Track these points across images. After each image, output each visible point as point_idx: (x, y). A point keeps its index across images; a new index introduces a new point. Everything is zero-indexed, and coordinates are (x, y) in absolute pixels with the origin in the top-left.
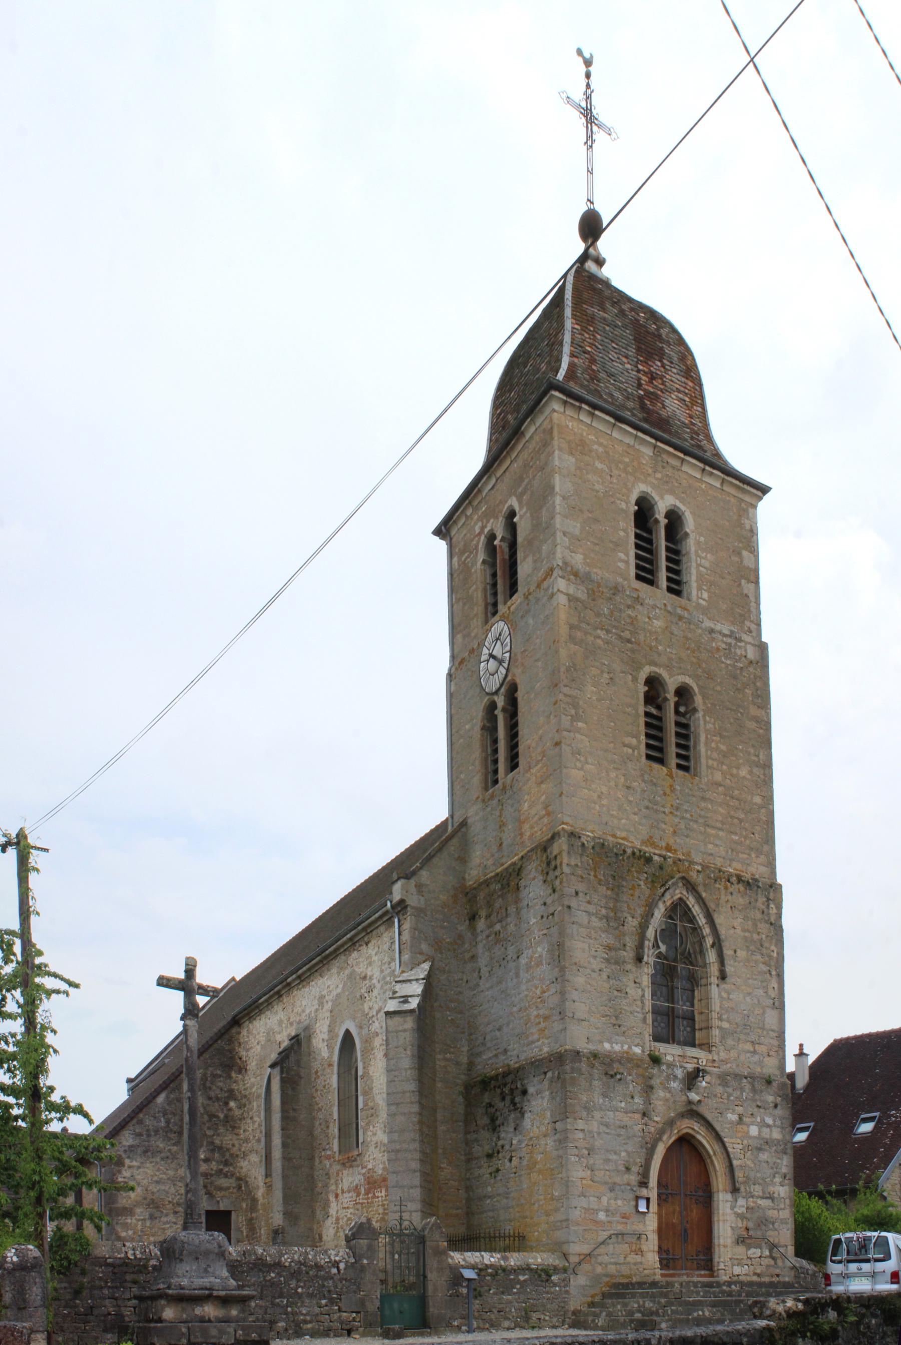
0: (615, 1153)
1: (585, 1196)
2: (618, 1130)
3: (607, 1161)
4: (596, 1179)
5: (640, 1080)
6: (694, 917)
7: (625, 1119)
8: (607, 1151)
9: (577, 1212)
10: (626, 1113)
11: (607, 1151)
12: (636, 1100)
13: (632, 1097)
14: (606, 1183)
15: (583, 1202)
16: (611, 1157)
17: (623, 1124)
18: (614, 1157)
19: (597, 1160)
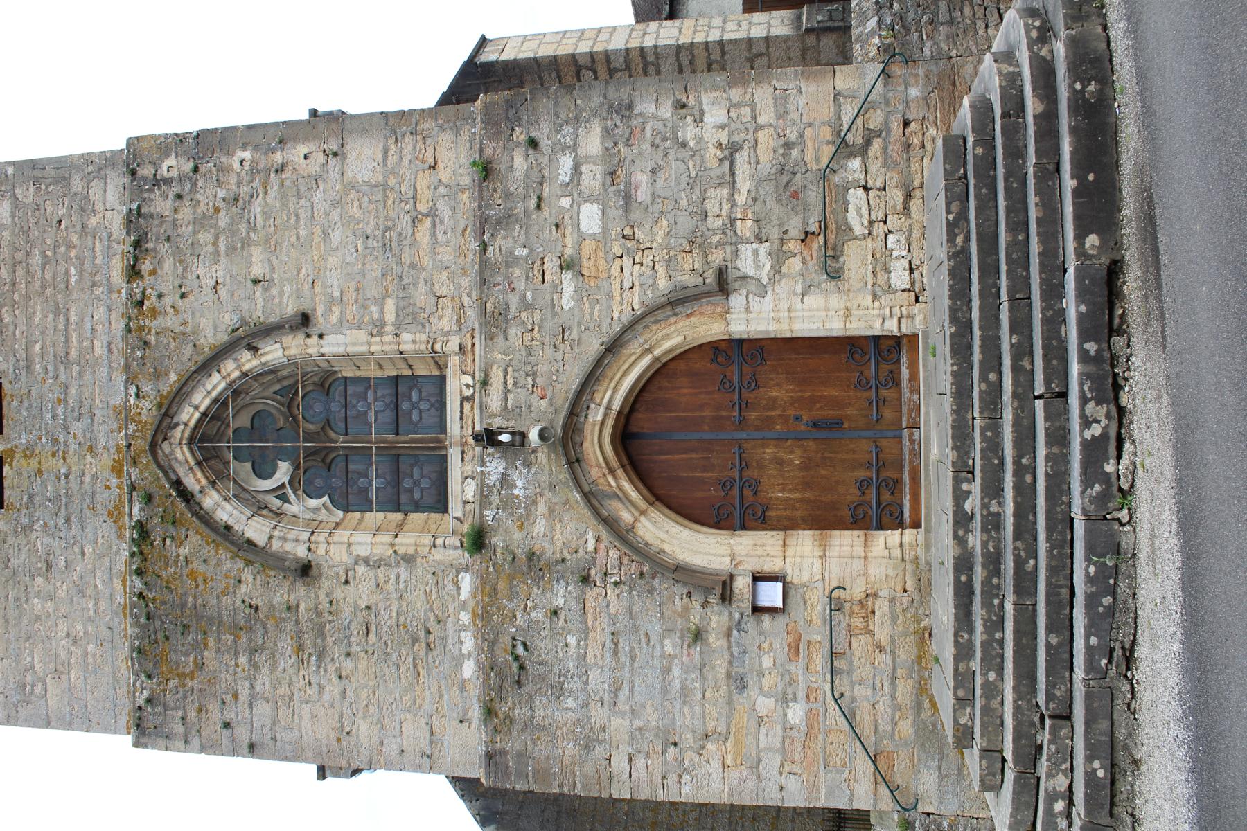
0: (668, 670)
1: (759, 760)
2: (623, 659)
3: (685, 693)
4: (722, 728)
5: (521, 588)
6: (215, 401)
7: (600, 634)
8: (665, 691)
9: (792, 784)
10: (586, 632)
11: (665, 691)
12: (560, 602)
13: (555, 613)
14: (729, 702)
15: (771, 763)
16: (677, 684)
17: (609, 645)
18: (676, 672)
19: (685, 721)
